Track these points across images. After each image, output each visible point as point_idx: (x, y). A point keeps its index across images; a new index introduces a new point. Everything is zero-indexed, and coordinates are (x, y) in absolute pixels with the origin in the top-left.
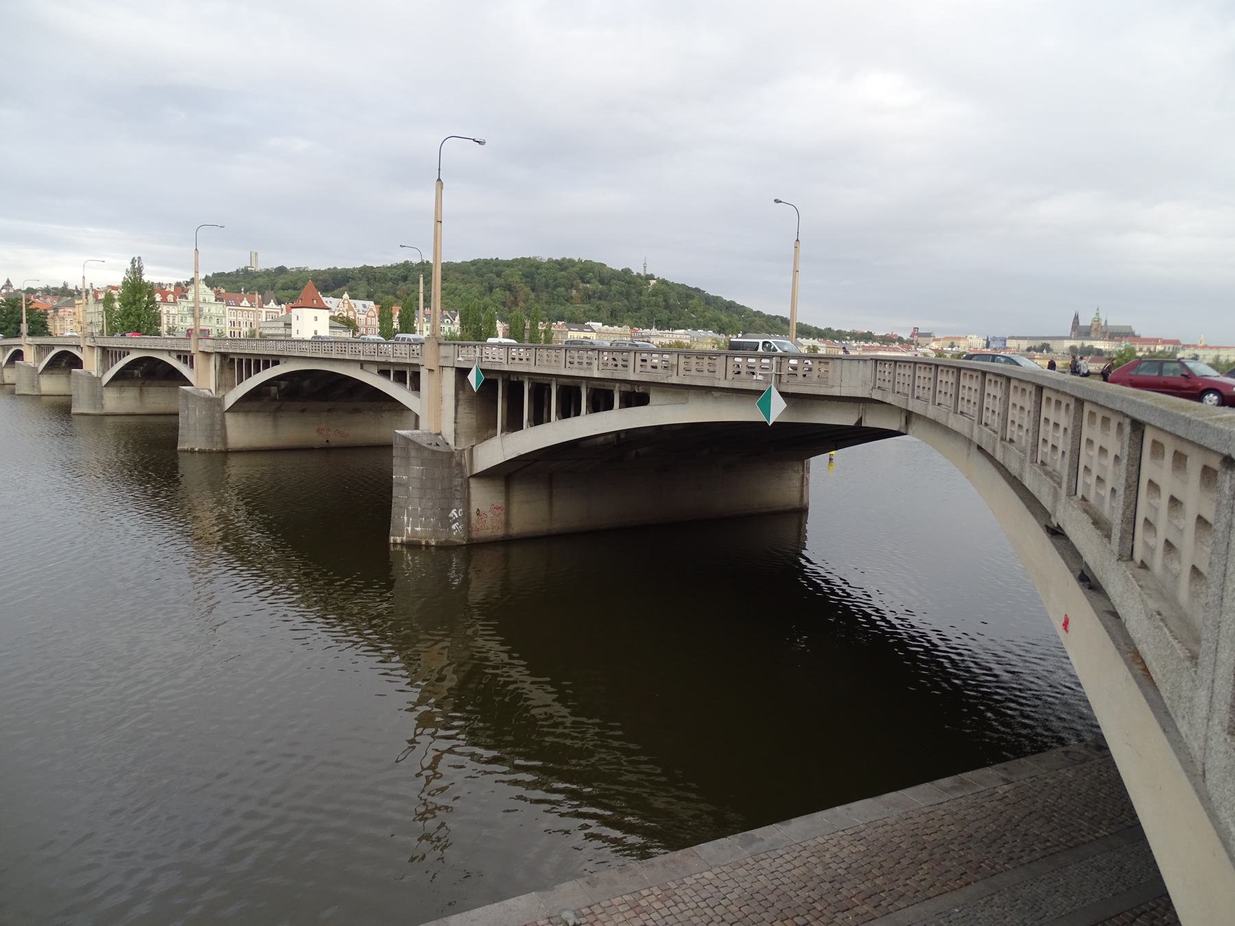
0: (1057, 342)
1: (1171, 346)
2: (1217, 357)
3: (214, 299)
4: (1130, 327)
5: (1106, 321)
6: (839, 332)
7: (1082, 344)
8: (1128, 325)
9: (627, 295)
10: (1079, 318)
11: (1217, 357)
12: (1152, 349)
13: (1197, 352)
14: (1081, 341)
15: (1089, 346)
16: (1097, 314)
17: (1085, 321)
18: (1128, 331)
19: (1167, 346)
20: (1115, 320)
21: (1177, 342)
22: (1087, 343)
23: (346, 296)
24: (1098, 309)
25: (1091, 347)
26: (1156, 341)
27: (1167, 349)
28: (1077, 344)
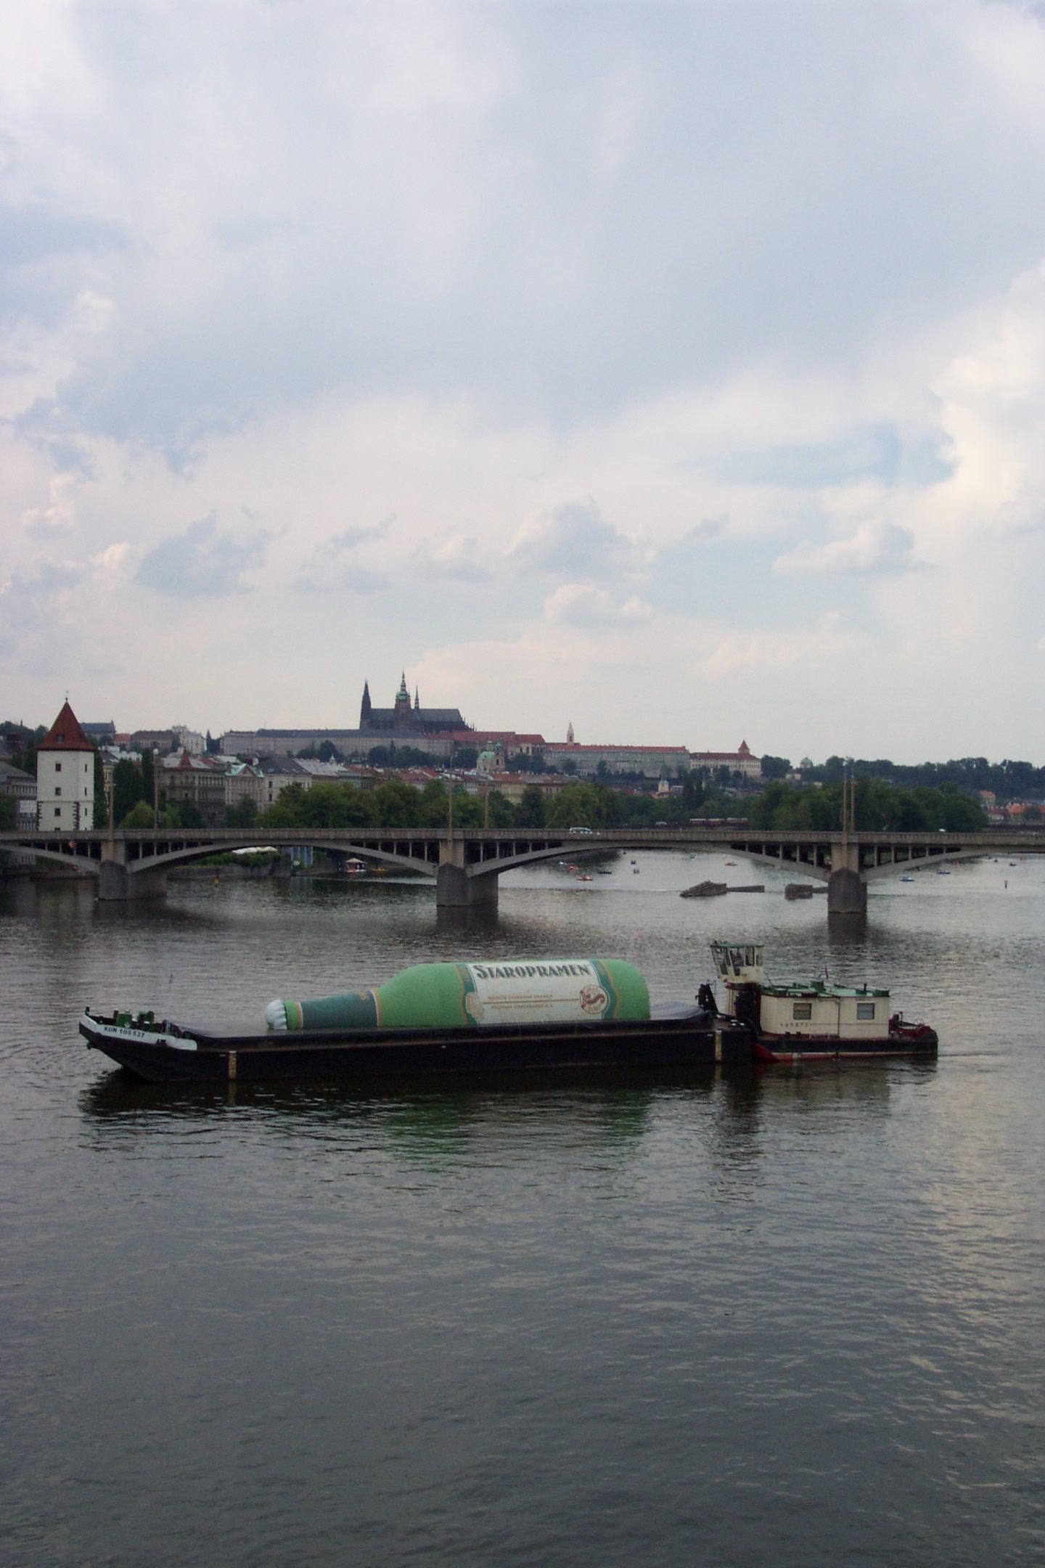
1: (530, 746)
2: (602, 765)
4: (456, 712)
5: (417, 703)
8: (455, 707)
10: (370, 695)
11: (602, 765)
14: (390, 739)
15: (404, 748)
16: (403, 686)
18: (455, 719)
19: (524, 746)
20: (430, 699)
21: (537, 739)
22: (400, 743)
24: (403, 677)
25: (407, 748)
27: (524, 751)
28: (384, 742)
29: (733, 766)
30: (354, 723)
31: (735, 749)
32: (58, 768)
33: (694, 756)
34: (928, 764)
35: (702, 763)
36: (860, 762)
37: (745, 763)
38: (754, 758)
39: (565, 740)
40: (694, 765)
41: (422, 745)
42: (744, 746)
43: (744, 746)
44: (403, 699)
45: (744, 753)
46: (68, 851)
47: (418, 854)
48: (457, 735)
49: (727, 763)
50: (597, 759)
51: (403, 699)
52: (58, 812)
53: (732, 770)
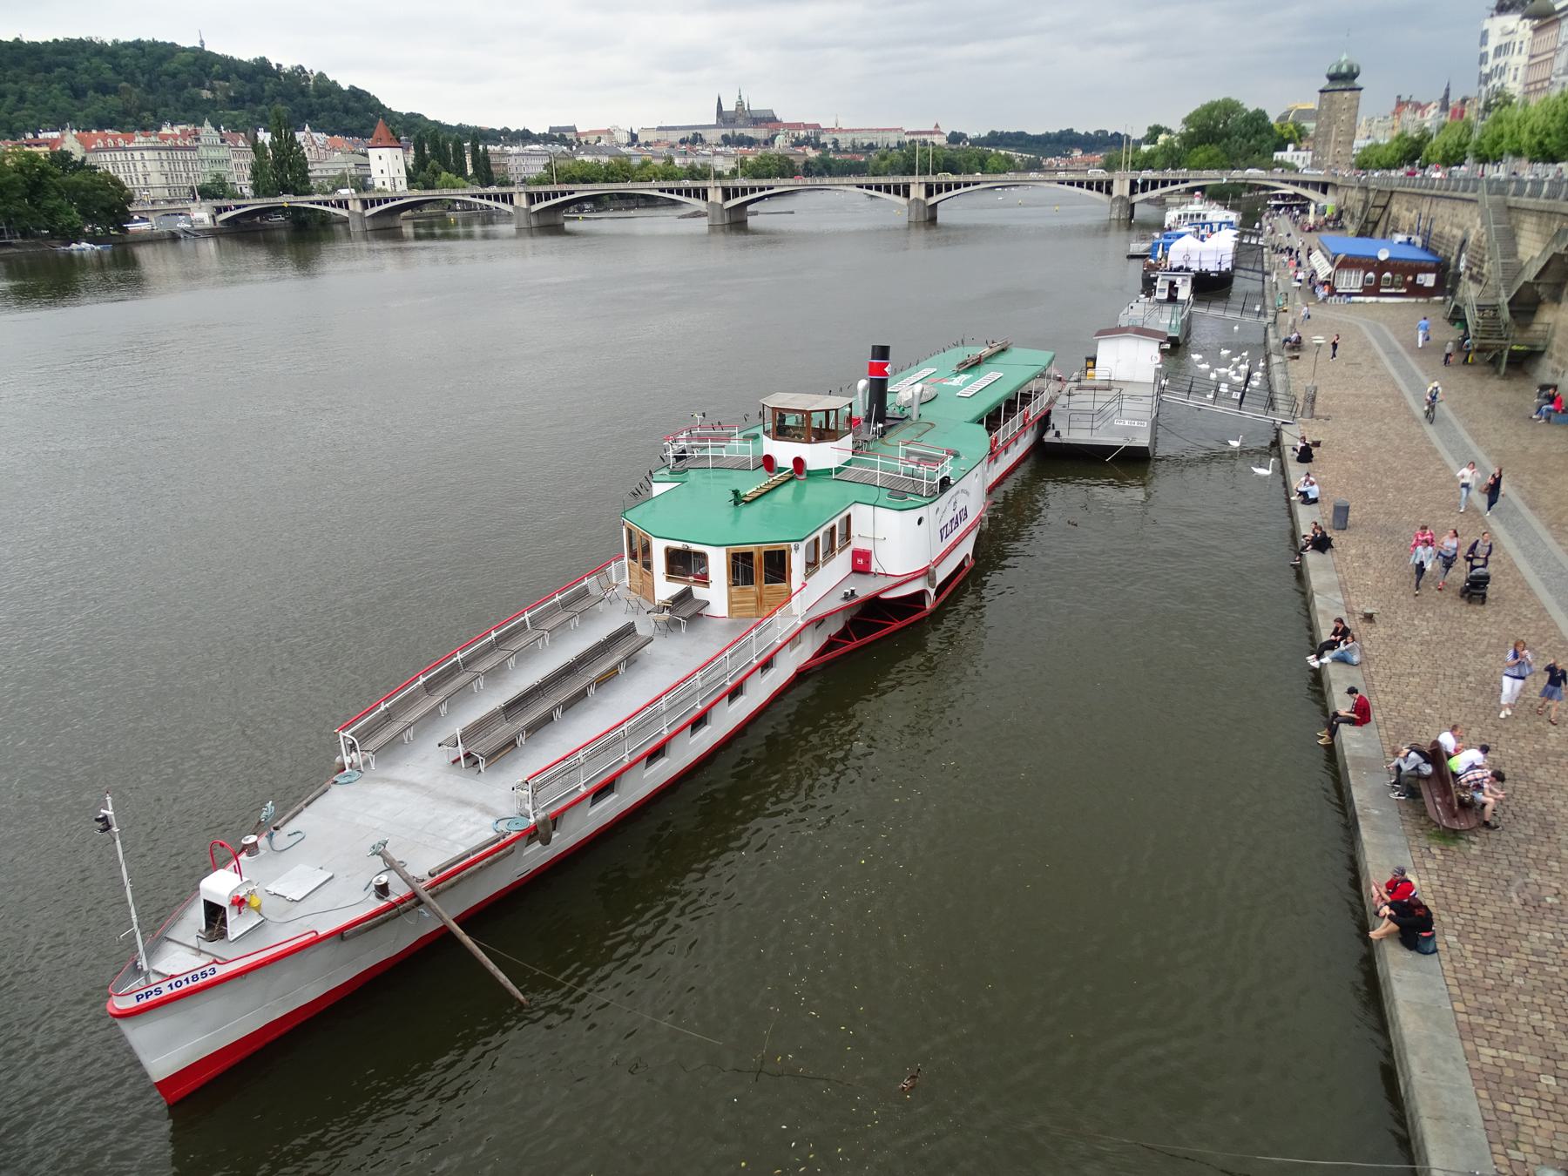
0: (708, 131)
2: (853, 141)
3: (219, 141)
6: (493, 130)
7: (733, 133)
9: (288, 97)
11: (853, 141)
12: (796, 135)
13: (835, 136)
16: (740, 97)
17: (729, 106)
19: (809, 131)
20: (757, 104)
21: (817, 126)
22: (738, 131)
23: (307, 128)
26: (798, 126)
28: (729, 132)
29: (929, 138)
31: (932, 129)
32: (380, 158)
33: (907, 133)
34: (1047, 133)
35: (912, 137)
36: (1008, 133)
37: (936, 136)
38: (942, 133)
40: (907, 139)
41: (749, 132)
42: (937, 126)
43: (937, 126)
44: (740, 104)
45: (937, 131)
46: (333, 206)
47: (504, 200)
49: (925, 137)
50: (850, 137)
52: (384, 183)
53: (929, 141)
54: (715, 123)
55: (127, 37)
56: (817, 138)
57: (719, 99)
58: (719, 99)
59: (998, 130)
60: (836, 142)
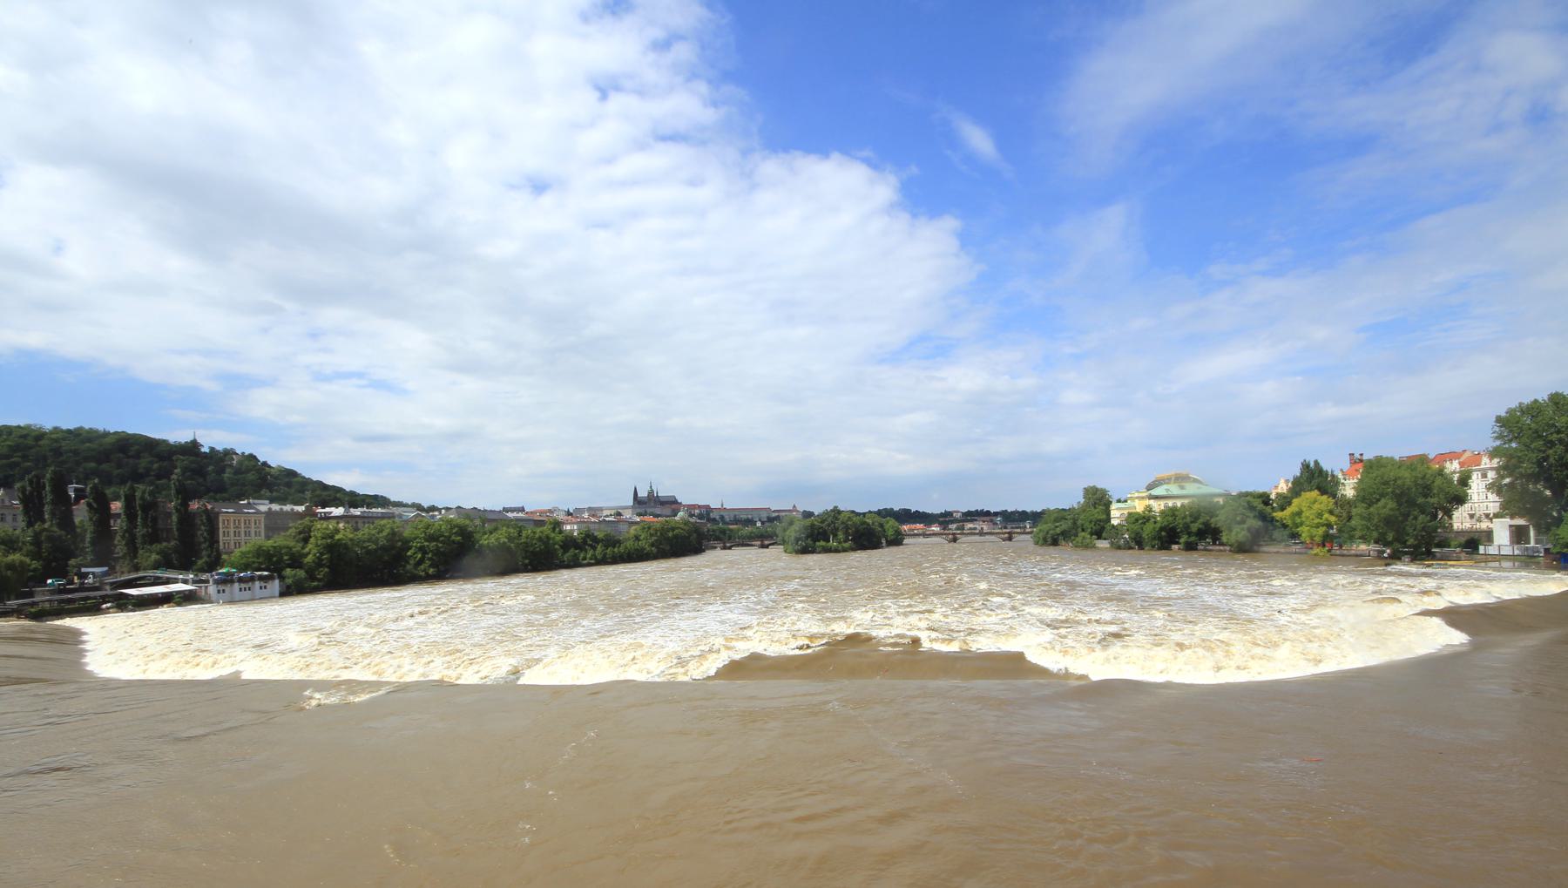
2: (735, 516)
4: (674, 497)
13: (722, 513)
20: (663, 492)
21: (708, 507)
30: (630, 502)
33: (774, 511)
35: (777, 514)
38: (798, 511)
39: (720, 507)
42: (794, 506)
43: (794, 506)
44: (651, 492)
45: (794, 508)
48: (674, 506)
51: (651, 492)
54: (632, 504)
55: (68, 424)
56: (708, 514)
57: (635, 489)
58: (635, 489)
59: (844, 506)
60: (722, 517)
